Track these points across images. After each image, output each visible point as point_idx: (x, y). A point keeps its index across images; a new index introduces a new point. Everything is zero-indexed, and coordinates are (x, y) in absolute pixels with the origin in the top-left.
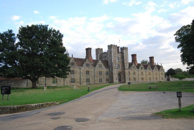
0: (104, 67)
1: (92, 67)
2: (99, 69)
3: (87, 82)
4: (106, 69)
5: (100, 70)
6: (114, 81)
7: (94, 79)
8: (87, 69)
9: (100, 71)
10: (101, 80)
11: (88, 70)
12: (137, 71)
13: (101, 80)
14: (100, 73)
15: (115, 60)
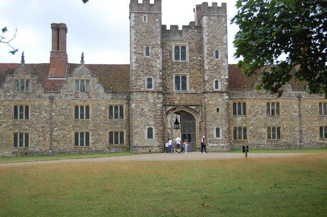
0: (101, 90)
1: (39, 92)
2: (76, 97)
3: (15, 145)
4: (109, 96)
5: (81, 100)
6: (136, 142)
7: (48, 135)
8: (20, 99)
9: (79, 104)
10: (81, 140)
11: (24, 104)
12: (296, 101)
13: (81, 140)
14: (82, 112)
15: (149, 60)
